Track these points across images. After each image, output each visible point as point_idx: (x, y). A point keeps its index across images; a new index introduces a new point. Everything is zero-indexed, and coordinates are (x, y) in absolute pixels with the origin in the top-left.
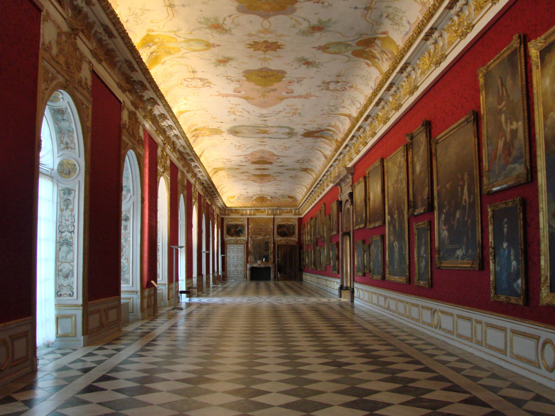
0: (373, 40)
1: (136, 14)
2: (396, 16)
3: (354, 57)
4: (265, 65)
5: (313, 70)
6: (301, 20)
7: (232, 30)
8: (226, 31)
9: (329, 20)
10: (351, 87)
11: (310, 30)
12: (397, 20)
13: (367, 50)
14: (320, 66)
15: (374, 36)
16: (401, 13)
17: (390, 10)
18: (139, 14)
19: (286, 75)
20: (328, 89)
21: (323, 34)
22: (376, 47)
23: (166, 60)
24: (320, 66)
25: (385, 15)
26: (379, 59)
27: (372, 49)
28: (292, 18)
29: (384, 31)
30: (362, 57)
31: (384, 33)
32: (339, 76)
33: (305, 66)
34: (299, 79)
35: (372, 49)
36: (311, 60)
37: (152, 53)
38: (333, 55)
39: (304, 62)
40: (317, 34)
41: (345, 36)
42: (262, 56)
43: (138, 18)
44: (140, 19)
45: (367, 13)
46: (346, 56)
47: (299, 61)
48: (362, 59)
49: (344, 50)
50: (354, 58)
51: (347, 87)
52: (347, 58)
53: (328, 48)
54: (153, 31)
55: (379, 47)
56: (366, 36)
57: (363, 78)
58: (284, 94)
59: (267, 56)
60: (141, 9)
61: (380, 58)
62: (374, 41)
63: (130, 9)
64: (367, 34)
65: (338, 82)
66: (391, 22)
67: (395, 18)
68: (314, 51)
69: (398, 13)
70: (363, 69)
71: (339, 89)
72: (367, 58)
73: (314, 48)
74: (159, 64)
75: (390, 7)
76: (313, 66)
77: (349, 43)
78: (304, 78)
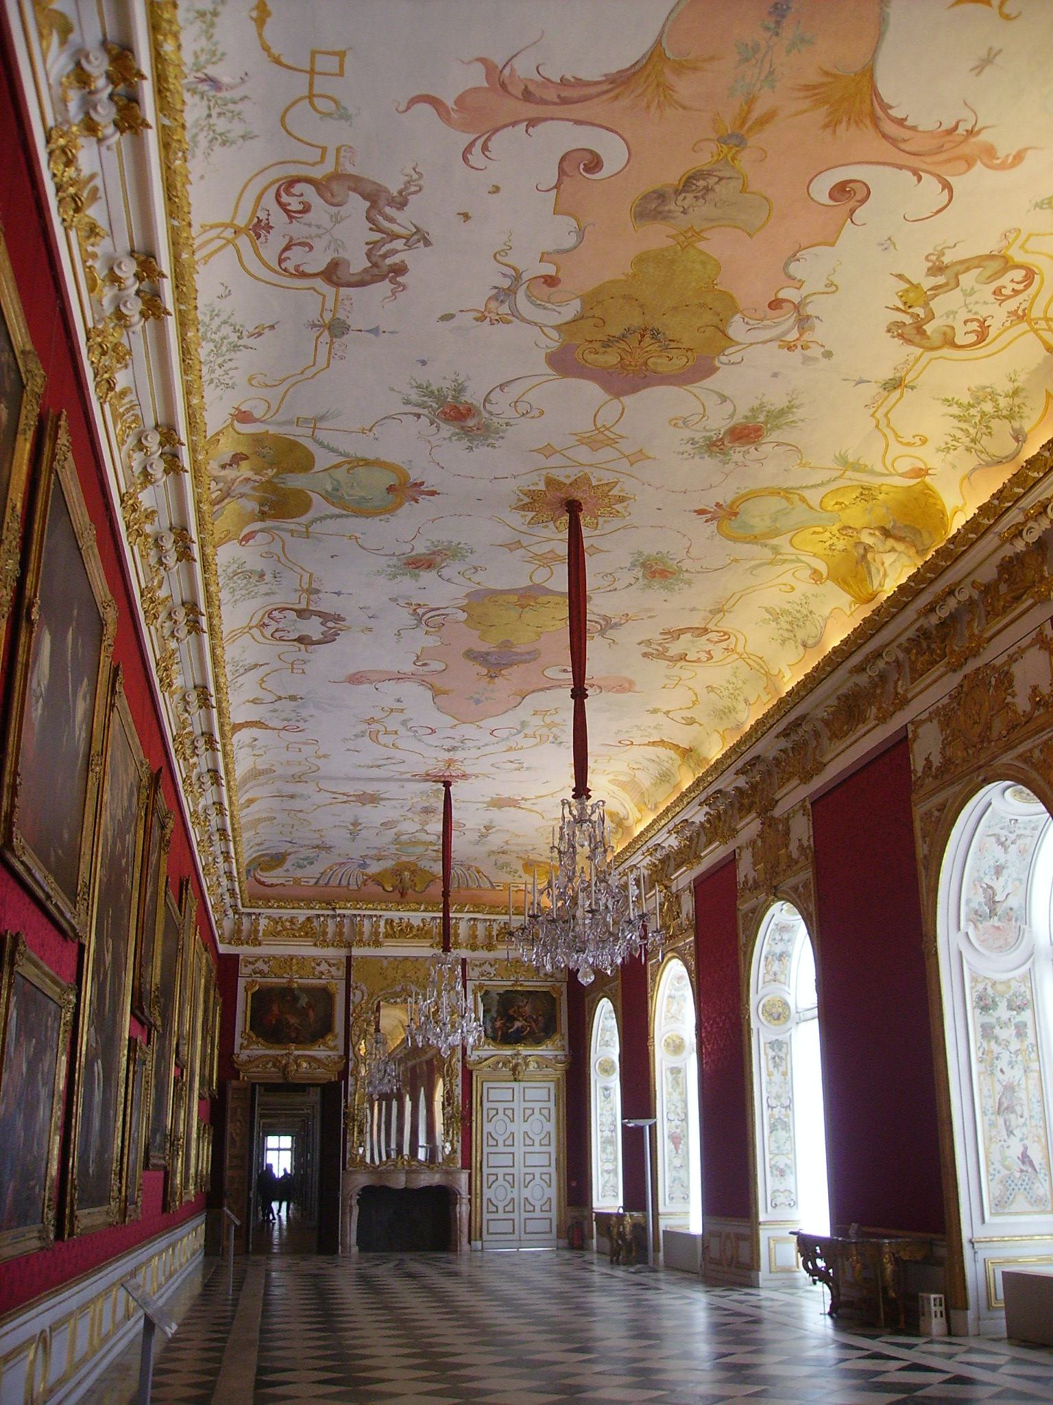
0: (266, 509)
1: (791, 623)
2: (246, 585)
3: (301, 440)
4: (610, 412)
5: (439, 377)
6: (460, 579)
7: (628, 565)
8: (643, 565)
9: (395, 577)
10: (259, 228)
11: (439, 559)
12: (239, 581)
13: (271, 472)
14: (414, 397)
15: (269, 523)
16: (238, 597)
17: (263, 588)
18: (790, 619)
19: (553, 341)
20: (374, 197)
21: (407, 548)
22: (246, 489)
23: (902, 475)
24: (414, 397)
25: (268, 577)
26: (223, 467)
27: (257, 478)
28: (479, 583)
29: (251, 542)
30: (277, 438)
31: (247, 538)
32: (337, 328)
33: (467, 397)
34: (504, 309)
35: (257, 478)
36: (447, 430)
37: (887, 533)
38: (371, 457)
39: (471, 423)
40: (421, 548)
41: (350, 538)
42: (606, 454)
43: (798, 615)
44: (798, 612)
45: (310, 583)
46: (333, 450)
47: (487, 427)
48: (272, 430)
49: (340, 474)
50: (300, 434)
51: (278, 218)
52: (320, 435)
53: (390, 489)
54: (815, 571)
55: (242, 496)
56: (292, 527)
57: (234, 337)
58: (613, 153)
59: (583, 454)
60: (776, 620)
61: (223, 473)
62: (262, 505)
63: (784, 641)
64: (292, 531)
65: (332, 274)
66: (248, 567)
67: (245, 581)
68: (431, 482)
69: (244, 592)
70: (249, 381)
71: (309, 191)
72: (257, 440)
73: (433, 493)
74: (927, 487)
75: (267, 594)
76: (439, 397)
77: (337, 511)
78: (481, 319)
